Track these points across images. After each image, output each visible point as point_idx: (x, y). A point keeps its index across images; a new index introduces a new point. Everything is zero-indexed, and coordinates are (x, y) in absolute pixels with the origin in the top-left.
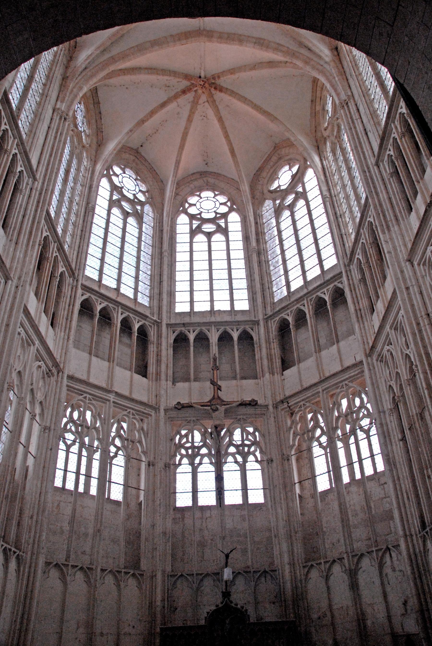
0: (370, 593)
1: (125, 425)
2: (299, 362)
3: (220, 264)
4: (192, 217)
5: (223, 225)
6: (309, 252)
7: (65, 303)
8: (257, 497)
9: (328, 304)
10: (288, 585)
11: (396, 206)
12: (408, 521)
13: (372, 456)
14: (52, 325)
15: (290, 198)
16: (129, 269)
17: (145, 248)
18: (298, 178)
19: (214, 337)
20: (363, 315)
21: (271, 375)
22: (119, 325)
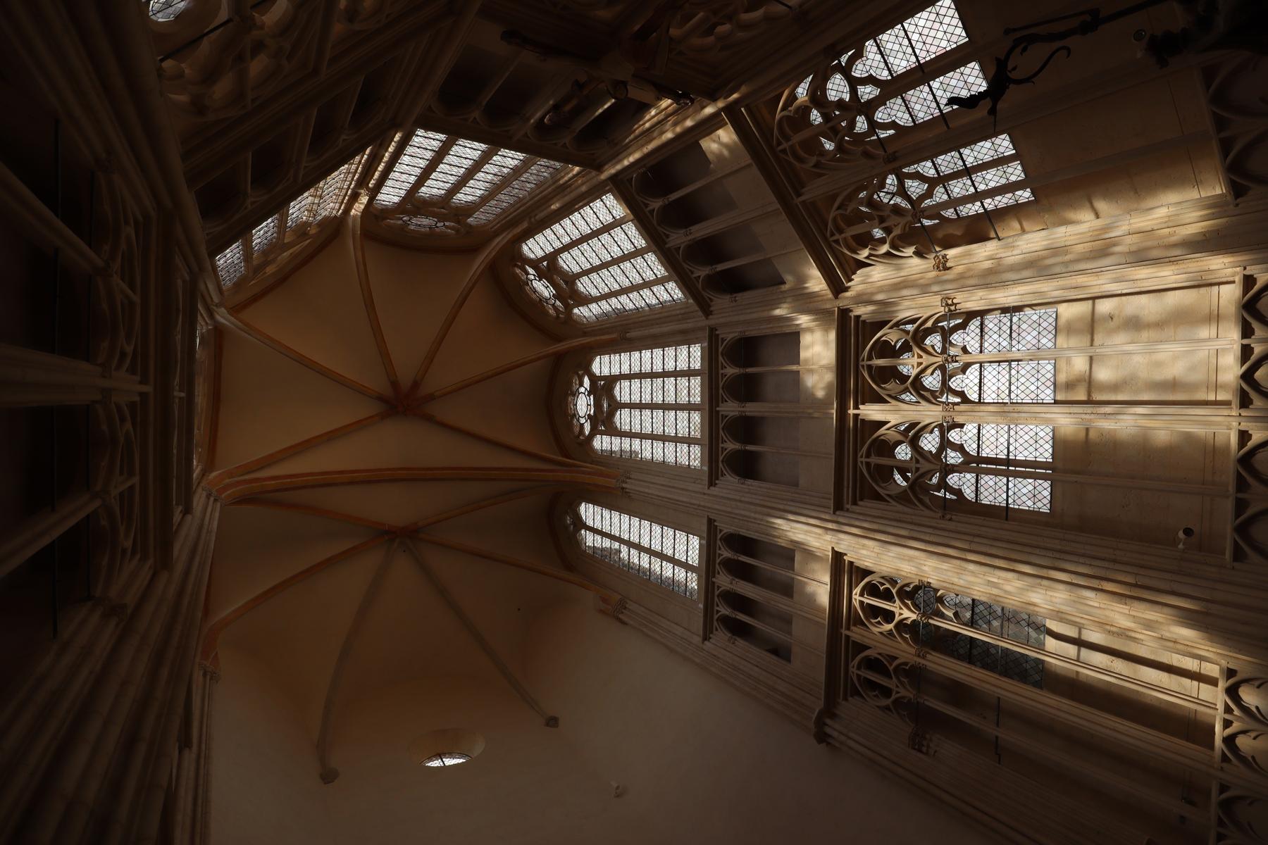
19: (731, 408)
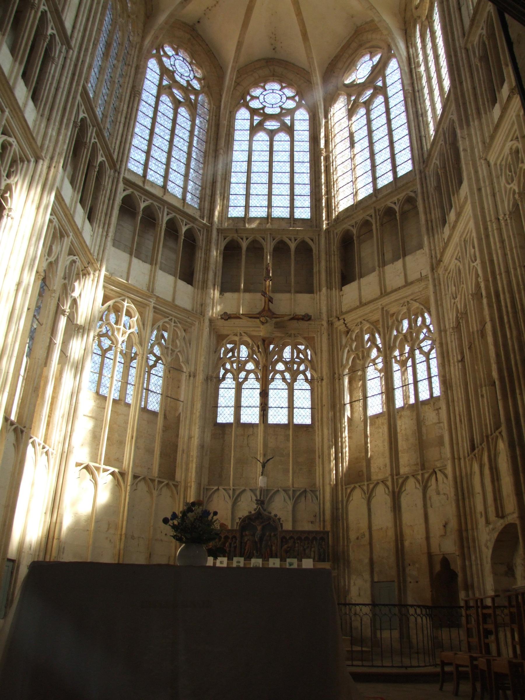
0: (412, 516)
1: (166, 335)
2: (361, 276)
3: (282, 167)
4: (254, 112)
5: (288, 123)
6: (383, 155)
7: (105, 197)
8: (303, 417)
9: (397, 214)
10: (328, 505)
11: (480, 97)
12: (458, 444)
13: (430, 378)
14: (89, 218)
15: (369, 93)
16: (178, 166)
17: (197, 144)
18: (379, 71)
19: (269, 247)
20: (434, 227)
21: (329, 290)
22: (164, 225)
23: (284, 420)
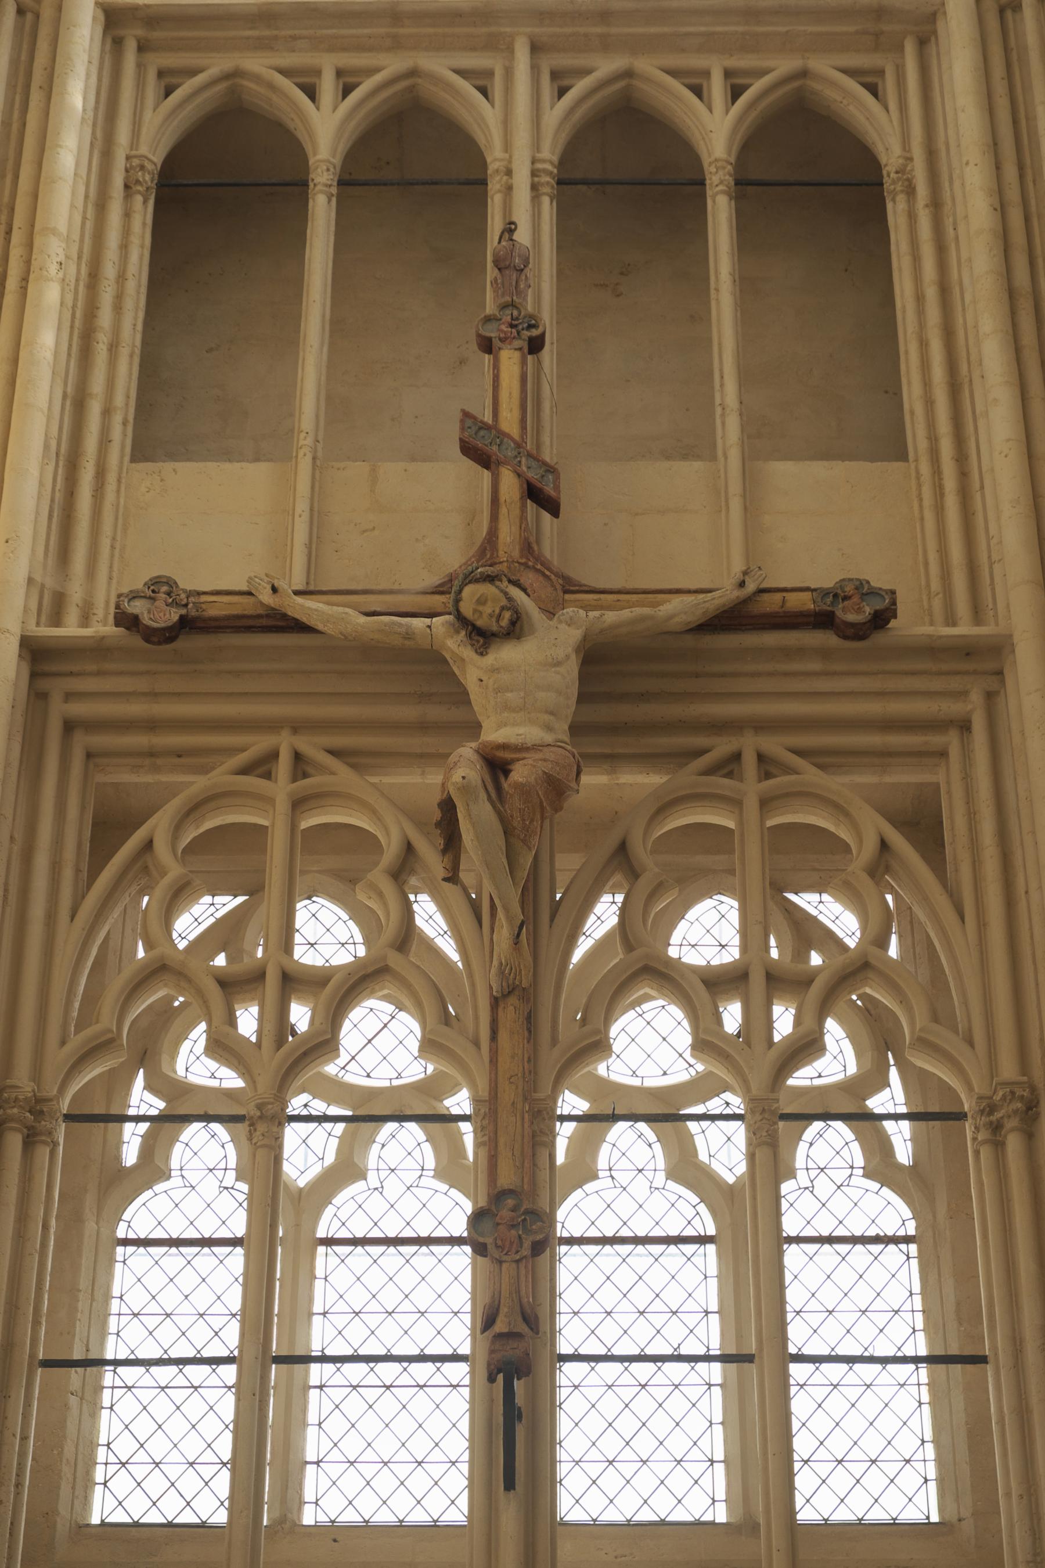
23: (701, 1496)
